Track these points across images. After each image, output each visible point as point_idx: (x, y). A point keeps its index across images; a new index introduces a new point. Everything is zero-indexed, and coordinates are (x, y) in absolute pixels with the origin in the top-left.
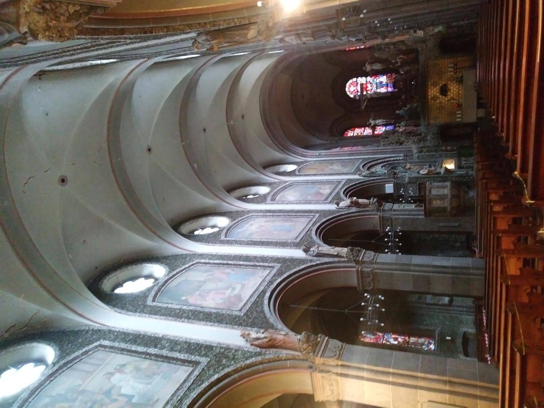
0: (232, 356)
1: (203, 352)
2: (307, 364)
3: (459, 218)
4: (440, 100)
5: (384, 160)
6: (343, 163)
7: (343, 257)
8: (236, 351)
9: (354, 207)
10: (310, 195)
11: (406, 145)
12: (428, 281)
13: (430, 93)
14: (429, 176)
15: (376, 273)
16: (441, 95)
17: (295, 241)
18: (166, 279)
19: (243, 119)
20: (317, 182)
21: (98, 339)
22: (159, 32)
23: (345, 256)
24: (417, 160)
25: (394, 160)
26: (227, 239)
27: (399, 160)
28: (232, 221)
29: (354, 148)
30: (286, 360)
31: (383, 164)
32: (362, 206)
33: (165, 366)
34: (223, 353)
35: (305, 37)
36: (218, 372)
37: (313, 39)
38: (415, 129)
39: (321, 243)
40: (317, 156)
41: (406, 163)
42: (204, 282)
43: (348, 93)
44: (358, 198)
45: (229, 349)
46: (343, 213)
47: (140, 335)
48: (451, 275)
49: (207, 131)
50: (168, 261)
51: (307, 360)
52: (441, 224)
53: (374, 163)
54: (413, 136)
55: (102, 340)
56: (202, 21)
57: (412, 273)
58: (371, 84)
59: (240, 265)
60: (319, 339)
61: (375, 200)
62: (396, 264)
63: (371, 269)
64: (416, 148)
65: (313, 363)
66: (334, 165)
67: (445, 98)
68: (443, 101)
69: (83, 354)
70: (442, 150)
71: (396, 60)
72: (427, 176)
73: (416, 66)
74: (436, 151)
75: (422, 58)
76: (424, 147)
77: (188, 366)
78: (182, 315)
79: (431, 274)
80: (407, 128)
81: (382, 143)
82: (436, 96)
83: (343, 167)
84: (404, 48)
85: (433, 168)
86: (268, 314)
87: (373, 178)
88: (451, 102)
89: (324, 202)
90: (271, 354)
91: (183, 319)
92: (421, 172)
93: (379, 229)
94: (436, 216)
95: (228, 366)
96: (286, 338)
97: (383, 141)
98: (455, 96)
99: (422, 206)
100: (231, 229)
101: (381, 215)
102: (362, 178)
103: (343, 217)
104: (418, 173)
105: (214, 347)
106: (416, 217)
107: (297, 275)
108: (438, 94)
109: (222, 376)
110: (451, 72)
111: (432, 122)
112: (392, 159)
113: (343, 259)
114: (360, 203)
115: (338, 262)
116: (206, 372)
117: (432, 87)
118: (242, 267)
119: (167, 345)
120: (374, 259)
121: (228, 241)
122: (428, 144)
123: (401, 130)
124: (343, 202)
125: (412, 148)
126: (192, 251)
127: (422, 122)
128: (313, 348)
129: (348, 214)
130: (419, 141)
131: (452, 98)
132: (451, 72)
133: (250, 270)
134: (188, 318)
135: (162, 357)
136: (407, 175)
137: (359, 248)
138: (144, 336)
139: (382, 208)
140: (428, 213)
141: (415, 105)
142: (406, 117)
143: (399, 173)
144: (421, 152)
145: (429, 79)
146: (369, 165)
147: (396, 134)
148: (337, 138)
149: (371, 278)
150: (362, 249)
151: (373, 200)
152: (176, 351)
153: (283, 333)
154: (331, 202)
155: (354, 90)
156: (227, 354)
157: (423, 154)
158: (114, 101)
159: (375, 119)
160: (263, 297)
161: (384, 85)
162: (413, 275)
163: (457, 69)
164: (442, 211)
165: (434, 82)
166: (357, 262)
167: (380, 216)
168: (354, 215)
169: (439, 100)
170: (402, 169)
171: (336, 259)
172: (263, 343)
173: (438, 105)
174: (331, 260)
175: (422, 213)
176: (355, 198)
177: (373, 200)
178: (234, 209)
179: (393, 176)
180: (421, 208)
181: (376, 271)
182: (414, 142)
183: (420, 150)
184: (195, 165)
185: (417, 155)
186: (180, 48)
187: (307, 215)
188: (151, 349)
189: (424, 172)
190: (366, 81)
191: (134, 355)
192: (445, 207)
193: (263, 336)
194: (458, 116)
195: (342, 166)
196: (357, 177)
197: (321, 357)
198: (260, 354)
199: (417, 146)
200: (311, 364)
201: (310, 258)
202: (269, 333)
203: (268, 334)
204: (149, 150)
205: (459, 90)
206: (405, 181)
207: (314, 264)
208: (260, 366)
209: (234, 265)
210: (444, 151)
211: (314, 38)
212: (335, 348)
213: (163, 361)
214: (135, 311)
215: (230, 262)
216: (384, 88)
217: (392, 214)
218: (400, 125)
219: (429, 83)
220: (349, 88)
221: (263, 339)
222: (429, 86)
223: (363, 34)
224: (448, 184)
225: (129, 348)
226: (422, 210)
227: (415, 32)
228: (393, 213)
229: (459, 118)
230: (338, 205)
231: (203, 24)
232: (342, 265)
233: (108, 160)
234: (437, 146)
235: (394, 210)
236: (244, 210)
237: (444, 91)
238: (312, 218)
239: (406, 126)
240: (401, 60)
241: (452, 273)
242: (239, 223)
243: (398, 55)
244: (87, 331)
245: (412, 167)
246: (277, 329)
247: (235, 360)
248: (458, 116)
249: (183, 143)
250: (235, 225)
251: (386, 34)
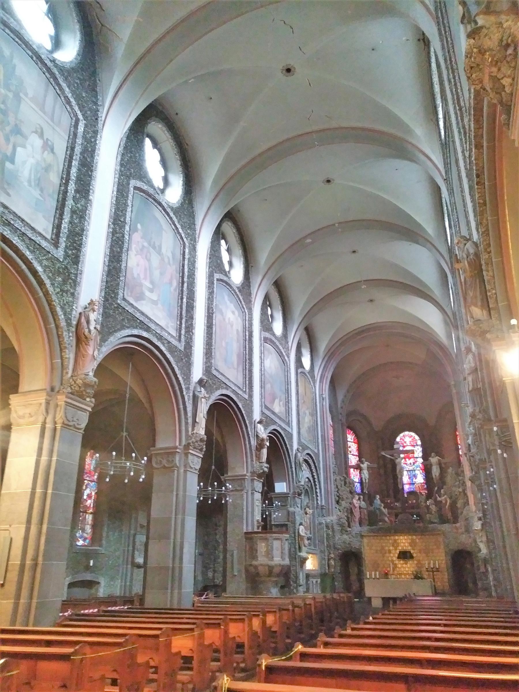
0: (66, 289)
1: (70, 252)
2: (57, 384)
3: (244, 576)
4: (393, 551)
5: (316, 480)
6: (313, 428)
7: (193, 430)
8: (73, 294)
9: (257, 442)
10: (272, 387)
11: (336, 508)
12: (164, 537)
13: (401, 537)
14: (297, 538)
15: (173, 471)
16: (400, 552)
17: (213, 368)
18: (163, 203)
19: (368, 301)
20: (288, 395)
21: (85, 118)
22: (478, 193)
23: (195, 432)
24: (317, 522)
25: (316, 492)
26: (215, 282)
27: (317, 500)
28: (238, 288)
29: (332, 443)
30: (62, 358)
31: (311, 479)
32: (258, 453)
33: (52, 204)
34: (69, 277)
35: (472, 379)
36: (45, 271)
37: (470, 388)
38: (357, 520)
39: (211, 402)
40: (321, 395)
41: (313, 508)
42: (159, 252)
43: (402, 435)
44: (268, 448)
45: (75, 285)
46: (249, 429)
47: (92, 171)
48: (171, 566)
49: (353, 255)
50: (186, 206)
51: (62, 384)
52: (235, 552)
53: (312, 468)
54: (348, 518)
55: (84, 122)
56: (492, 248)
57: (174, 516)
58: (414, 463)
59: (182, 299)
60: (88, 399)
61: (266, 470)
62: (185, 496)
63: (178, 465)
64: (332, 521)
65: (58, 392)
66: (310, 418)
68: (392, 555)
69: (66, 97)
70: (330, 554)
72: (297, 535)
73: (436, 521)
74: (329, 546)
75: (446, 527)
76: (333, 531)
77: (52, 234)
78: (118, 224)
79: (172, 541)
80: (358, 509)
81: (338, 478)
83: (307, 429)
84: (459, 504)
85: (306, 542)
86: (120, 334)
87: (293, 466)
88: (391, 564)
89: (263, 404)
90: (69, 338)
91: (112, 226)
92: (301, 527)
93: (229, 474)
94: (246, 546)
95: (53, 284)
96: (89, 358)
97: (340, 479)
98: (398, 569)
99: (258, 528)
100: (228, 287)
101: (247, 477)
102: (294, 452)
103: (244, 429)
104: (301, 524)
105: (78, 266)
106: (245, 521)
107: (170, 371)
109: (40, 276)
110: (429, 564)
111: (365, 540)
112: (318, 490)
113: (190, 429)
114: (262, 450)
115: (187, 423)
116: (44, 256)
117: (409, 541)
118: (180, 301)
119: (79, 205)
120: (192, 468)
121: (213, 283)
122: (338, 536)
123: (355, 501)
124: (262, 428)
125: (333, 516)
126: (199, 237)
127: (365, 528)
128: (77, 391)
129: (248, 434)
130: (341, 525)
131: (395, 567)
132: (429, 564)
133: (175, 311)
134: (114, 233)
135: (64, 199)
136: (298, 510)
137: (204, 449)
138: (90, 176)
139: (255, 478)
140: (249, 536)
141: (386, 519)
142: (372, 508)
143: (300, 500)
144: (327, 527)
145: (419, 537)
146: (310, 461)
147: (350, 496)
148: (344, 420)
149: (166, 465)
150: (203, 453)
151: (265, 467)
152: (72, 217)
153: (96, 353)
154: (263, 413)
155: (405, 442)
156: (68, 283)
157: (325, 529)
158: (390, 135)
159: (368, 468)
160: (141, 328)
161: (412, 480)
162: (170, 519)
163: (433, 572)
164: (253, 553)
166: (187, 447)
167: (245, 475)
168: (247, 443)
170: (305, 504)
171: (190, 421)
172: (83, 328)
173: (387, 548)
174: (190, 414)
175: (250, 530)
176: (268, 444)
177: (265, 467)
178: (254, 290)
179: (296, 491)
180: (256, 527)
181: (176, 471)
182: (339, 520)
183: (330, 526)
184: (309, 241)
185: (324, 522)
186: (458, 220)
187: (246, 383)
188: (74, 185)
189: (302, 530)
190: (417, 458)
191: (66, 164)
192: (257, 557)
193: (92, 328)
194: (373, 573)
195: (309, 428)
196: (295, 446)
197: (66, 402)
198: (69, 324)
199: (335, 521)
200: (57, 389)
201: (192, 388)
202: (96, 336)
203: (94, 335)
204: (328, 181)
205: (405, 574)
206: (291, 507)
207: (184, 393)
208: (53, 325)
209: (182, 291)
210: (328, 556)
211: (472, 391)
212: (77, 419)
213: (58, 201)
214: (122, 165)
215: (185, 285)
216: (409, 480)
217: (248, 490)
218: (362, 500)
219: (414, 537)
220: (407, 435)
221: (88, 328)
222: (410, 537)
223: (477, 454)
224: (287, 562)
225: (74, 158)
226: (253, 528)
227: (480, 519)
228: (250, 493)
229: (371, 575)
230: (258, 423)
231: (488, 250)
232: (183, 428)
233: (315, 128)
234: (335, 548)
235: (252, 494)
236: (252, 302)
237: (405, 555)
238: (242, 390)
239: (360, 508)
240: (444, 502)
241: (173, 568)
242: (236, 296)
243: (451, 498)
244: (96, 104)
245: (308, 515)
246: (101, 346)
247: (61, 293)
248: (373, 573)
249: (337, 225)
250: (233, 292)
251: (477, 483)
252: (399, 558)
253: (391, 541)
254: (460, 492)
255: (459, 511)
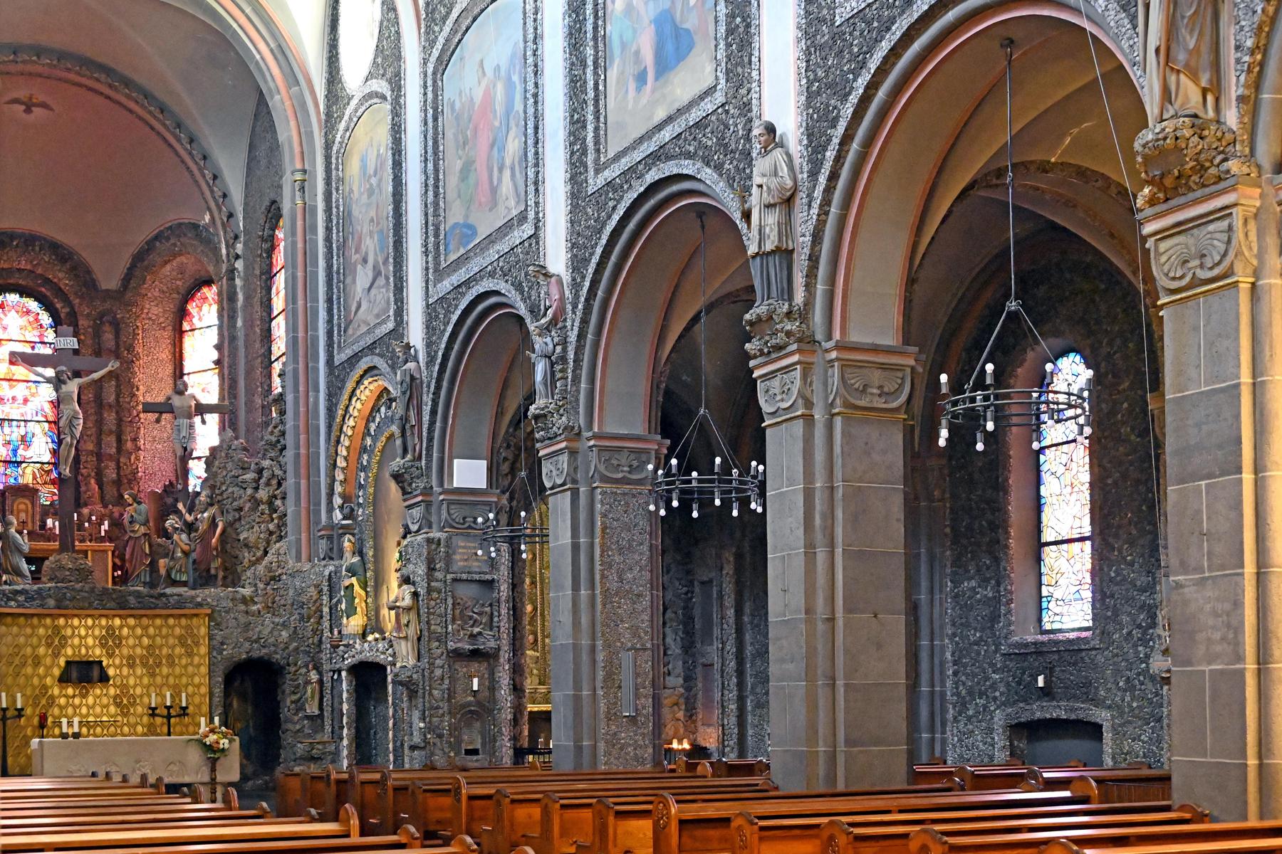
4: (48, 661)
13: (76, 622)
16: (68, 663)
67: (52, 676)
68: (41, 670)
71: (212, 505)
73: (184, 578)
82: (63, 647)
108: (69, 651)
145: (131, 621)
161: (15, 451)
163: (169, 717)
165: (120, 638)
169: (45, 655)
219: (117, 622)
222: (104, 622)
240: (202, 527)
252: (64, 679)
253: (41, 631)
254: (256, 503)
255: (247, 556)
